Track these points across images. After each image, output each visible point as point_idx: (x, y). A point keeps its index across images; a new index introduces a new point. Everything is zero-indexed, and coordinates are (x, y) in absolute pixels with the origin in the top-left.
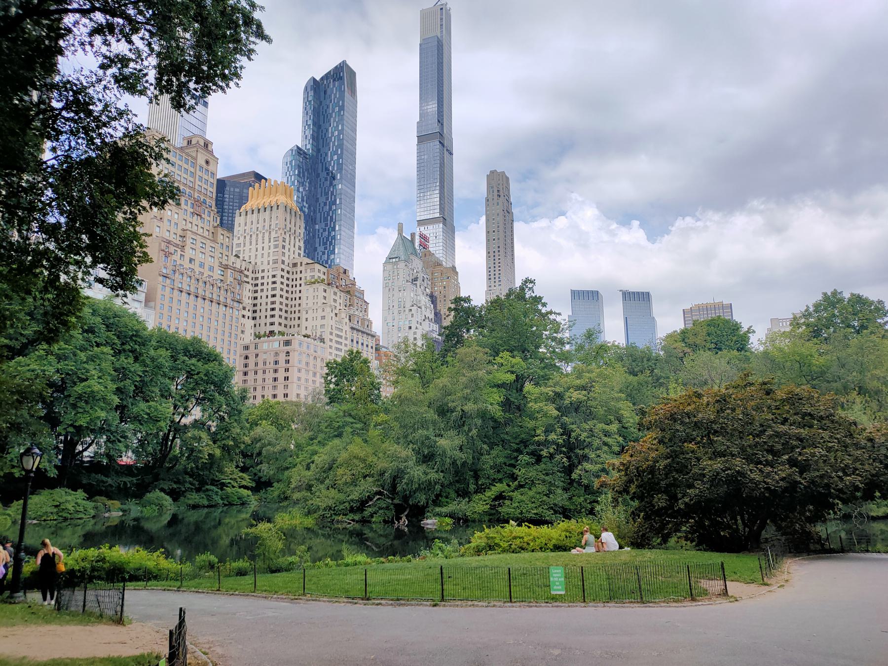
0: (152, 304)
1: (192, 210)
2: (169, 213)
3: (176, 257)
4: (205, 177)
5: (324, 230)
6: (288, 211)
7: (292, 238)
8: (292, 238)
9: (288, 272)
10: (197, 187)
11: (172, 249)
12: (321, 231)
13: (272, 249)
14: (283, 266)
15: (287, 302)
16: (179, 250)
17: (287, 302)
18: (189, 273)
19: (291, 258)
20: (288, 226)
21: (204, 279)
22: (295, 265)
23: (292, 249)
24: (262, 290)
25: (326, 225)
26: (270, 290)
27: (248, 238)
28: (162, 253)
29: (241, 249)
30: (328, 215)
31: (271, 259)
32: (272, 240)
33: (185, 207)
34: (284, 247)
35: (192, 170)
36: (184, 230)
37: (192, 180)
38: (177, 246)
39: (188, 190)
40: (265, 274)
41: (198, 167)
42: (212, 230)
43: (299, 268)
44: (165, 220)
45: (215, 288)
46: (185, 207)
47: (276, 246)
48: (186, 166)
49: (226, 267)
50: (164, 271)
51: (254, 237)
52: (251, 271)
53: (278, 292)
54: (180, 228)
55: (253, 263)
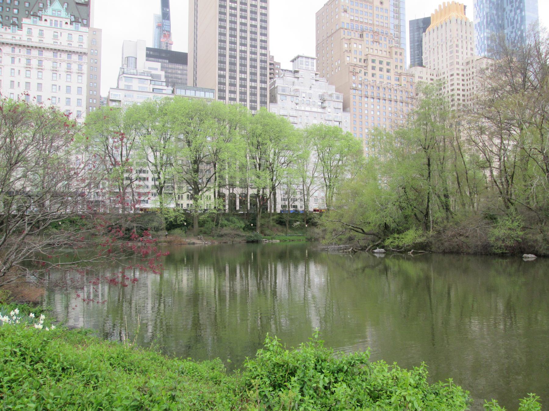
0: (348, 109)
1: (372, 40)
2: (355, 46)
3: (362, 74)
4: (381, 14)
5: (512, 32)
6: (459, 22)
7: (464, 43)
8: (464, 43)
9: (463, 70)
10: (376, 23)
11: (358, 70)
12: (509, 33)
13: (449, 55)
14: (458, 66)
15: (463, 93)
16: (363, 70)
17: (463, 93)
18: (372, 84)
19: (465, 58)
20: (460, 34)
21: (383, 86)
22: (468, 63)
23: (465, 51)
24: (444, 88)
25: (513, 28)
26: (449, 86)
27: (432, 51)
28: (351, 74)
29: (428, 61)
30: (514, 19)
31: (449, 62)
32: (448, 48)
33: (367, 39)
34: (457, 52)
35: (371, 11)
36: (367, 55)
37: (371, 18)
38: (361, 67)
39: (369, 27)
40: (445, 76)
41: (375, 8)
42: (388, 50)
43: (470, 65)
44: (353, 52)
45: (392, 91)
46: (367, 39)
47: (451, 52)
48: (366, 10)
49: (400, 75)
50: (354, 86)
51: (436, 49)
52: (435, 75)
53: (456, 87)
54: (363, 54)
55: (437, 69)
